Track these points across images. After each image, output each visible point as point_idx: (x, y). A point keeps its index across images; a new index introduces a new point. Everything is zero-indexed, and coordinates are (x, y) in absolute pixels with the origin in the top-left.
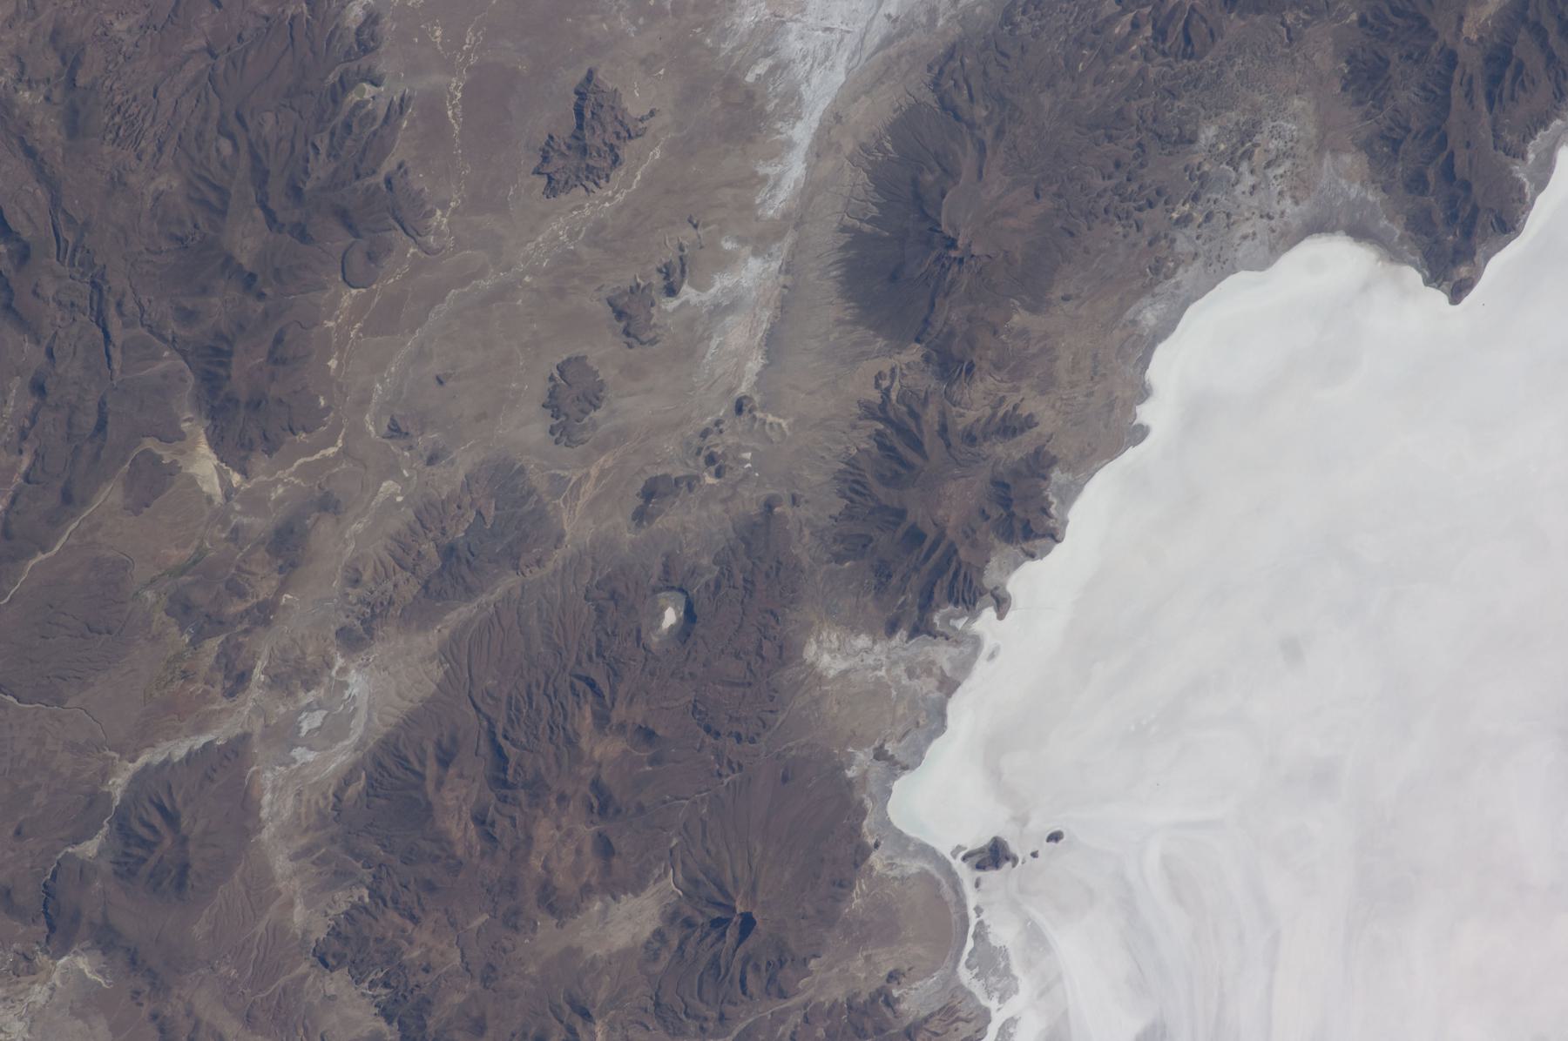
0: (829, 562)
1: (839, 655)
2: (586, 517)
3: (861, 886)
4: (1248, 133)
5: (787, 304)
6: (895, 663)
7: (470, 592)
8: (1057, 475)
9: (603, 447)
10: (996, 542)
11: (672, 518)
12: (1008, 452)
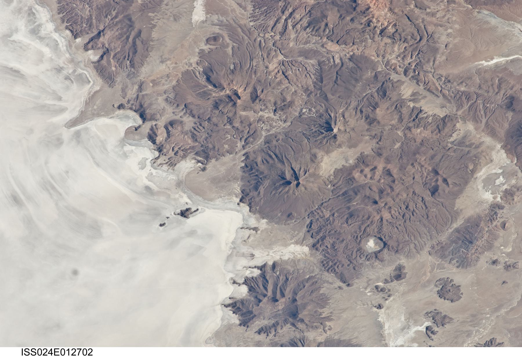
0: (315, 275)
1: (293, 251)
2: (422, 262)
3: (238, 190)
6: (268, 255)
7: (457, 230)
8: (235, 319)
9: (429, 281)
10: (249, 298)
11: (389, 270)
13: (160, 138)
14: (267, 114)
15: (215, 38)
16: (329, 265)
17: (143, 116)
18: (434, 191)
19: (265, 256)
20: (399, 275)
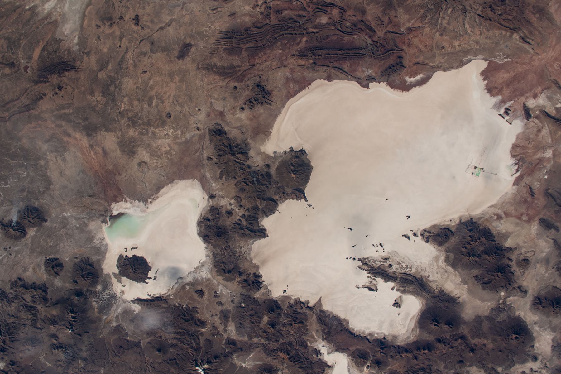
1: (257, 295)
2: (230, 307)
4: (240, 247)
5: (224, 286)
8: (257, 273)
11: (236, 301)
12: (252, 275)
13: (302, 305)
14: (286, 321)
15: (307, 330)
16: (248, 296)
17: (308, 307)
18: (241, 324)
19: (262, 291)
20: (232, 301)
